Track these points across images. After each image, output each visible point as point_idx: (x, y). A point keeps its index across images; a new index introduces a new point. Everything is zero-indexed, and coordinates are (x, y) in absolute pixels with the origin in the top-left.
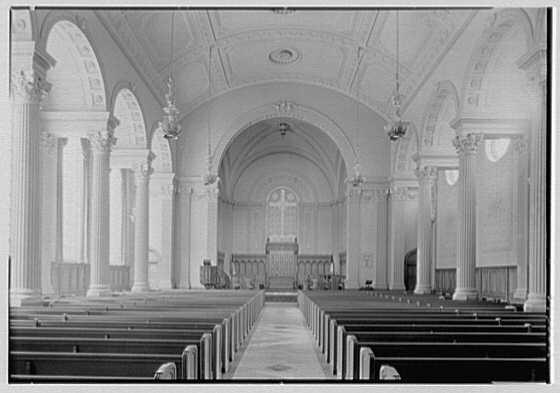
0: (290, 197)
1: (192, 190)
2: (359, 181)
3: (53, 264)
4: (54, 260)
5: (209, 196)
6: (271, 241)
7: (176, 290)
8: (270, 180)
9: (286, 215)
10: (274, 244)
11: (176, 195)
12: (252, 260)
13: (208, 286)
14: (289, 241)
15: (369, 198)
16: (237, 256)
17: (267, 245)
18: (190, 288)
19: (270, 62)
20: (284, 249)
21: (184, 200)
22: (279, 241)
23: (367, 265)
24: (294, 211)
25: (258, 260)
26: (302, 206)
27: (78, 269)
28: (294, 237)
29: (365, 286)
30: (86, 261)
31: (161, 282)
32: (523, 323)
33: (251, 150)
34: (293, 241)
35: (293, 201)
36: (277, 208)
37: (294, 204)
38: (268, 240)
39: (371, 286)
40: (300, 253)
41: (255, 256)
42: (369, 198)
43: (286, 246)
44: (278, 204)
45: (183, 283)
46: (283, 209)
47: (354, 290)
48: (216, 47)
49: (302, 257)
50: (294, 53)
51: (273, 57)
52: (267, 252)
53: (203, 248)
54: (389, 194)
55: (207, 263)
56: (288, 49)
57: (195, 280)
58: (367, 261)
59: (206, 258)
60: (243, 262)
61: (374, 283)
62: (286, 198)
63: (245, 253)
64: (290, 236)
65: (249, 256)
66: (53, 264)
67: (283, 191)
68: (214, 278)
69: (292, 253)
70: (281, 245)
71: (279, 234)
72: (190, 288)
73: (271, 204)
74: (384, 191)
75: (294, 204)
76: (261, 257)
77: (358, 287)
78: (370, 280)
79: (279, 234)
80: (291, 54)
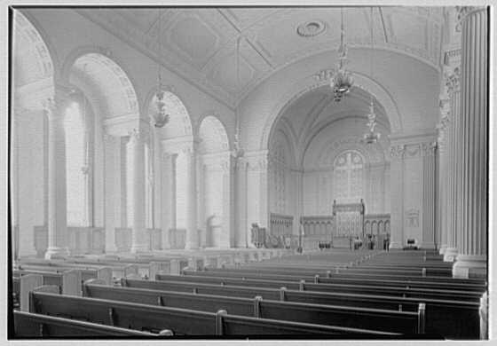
0: (357, 159)
1: (248, 164)
2: (372, 138)
3: (116, 229)
4: (171, 226)
5: (261, 167)
6: (337, 203)
7: (233, 249)
8: (337, 145)
9: (352, 177)
10: (338, 206)
11: (235, 170)
12: (309, 222)
13: (231, 247)
14: (354, 202)
15: (415, 153)
16: (305, 218)
17: (334, 207)
18: (247, 247)
19: (299, 37)
20: (350, 211)
21: (241, 172)
22: (346, 202)
23: (412, 222)
24: (361, 173)
25: (309, 222)
26: (369, 167)
27: (78, 234)
28: (360, 197)
29: (407, 245)
30: (158, 226)
31: (222, 243)
32: (279, 286)
33: (312, 123)
34: (359, 202)
35: (359, 163)
36: (344, 171)
37: (361, 166)
38: (335, 202)
39: (413, 245)
40: (366, 213)
41: (323, 218)
42: (415, 153)
43: (353, 207)
44: (345, 168)
45: (242, 244)
46: (349, 172)
47: (399, 249)
48: (244, 39)
49: (369, 217)
50: (320, 24)
51: (315, 27)
52: (334, 214)
53: (257, 213)
54: (436, 147)
55: (255, 226)
56: (316, 22)
57: (248, 242)
58: (412, 219)
59: (255, 222)
60: (323, 223)
61: (416, 242)
62: (352, 160)
63: (315, 215)
64: (357, 197)
65: (317, 218)
66: (116, 229)
67: (350, 155)
68: (261, 237)
69: (358, 213)
70: (348, 206)
71: (345, 196)
72: (247, 247)
73: (338, 168)
74: (431, 144)
75: (361, 166)
76: (329, 218)
77: (402, 247)
78: (411, 239)
79: (345, 196)
80: (317, 25)
